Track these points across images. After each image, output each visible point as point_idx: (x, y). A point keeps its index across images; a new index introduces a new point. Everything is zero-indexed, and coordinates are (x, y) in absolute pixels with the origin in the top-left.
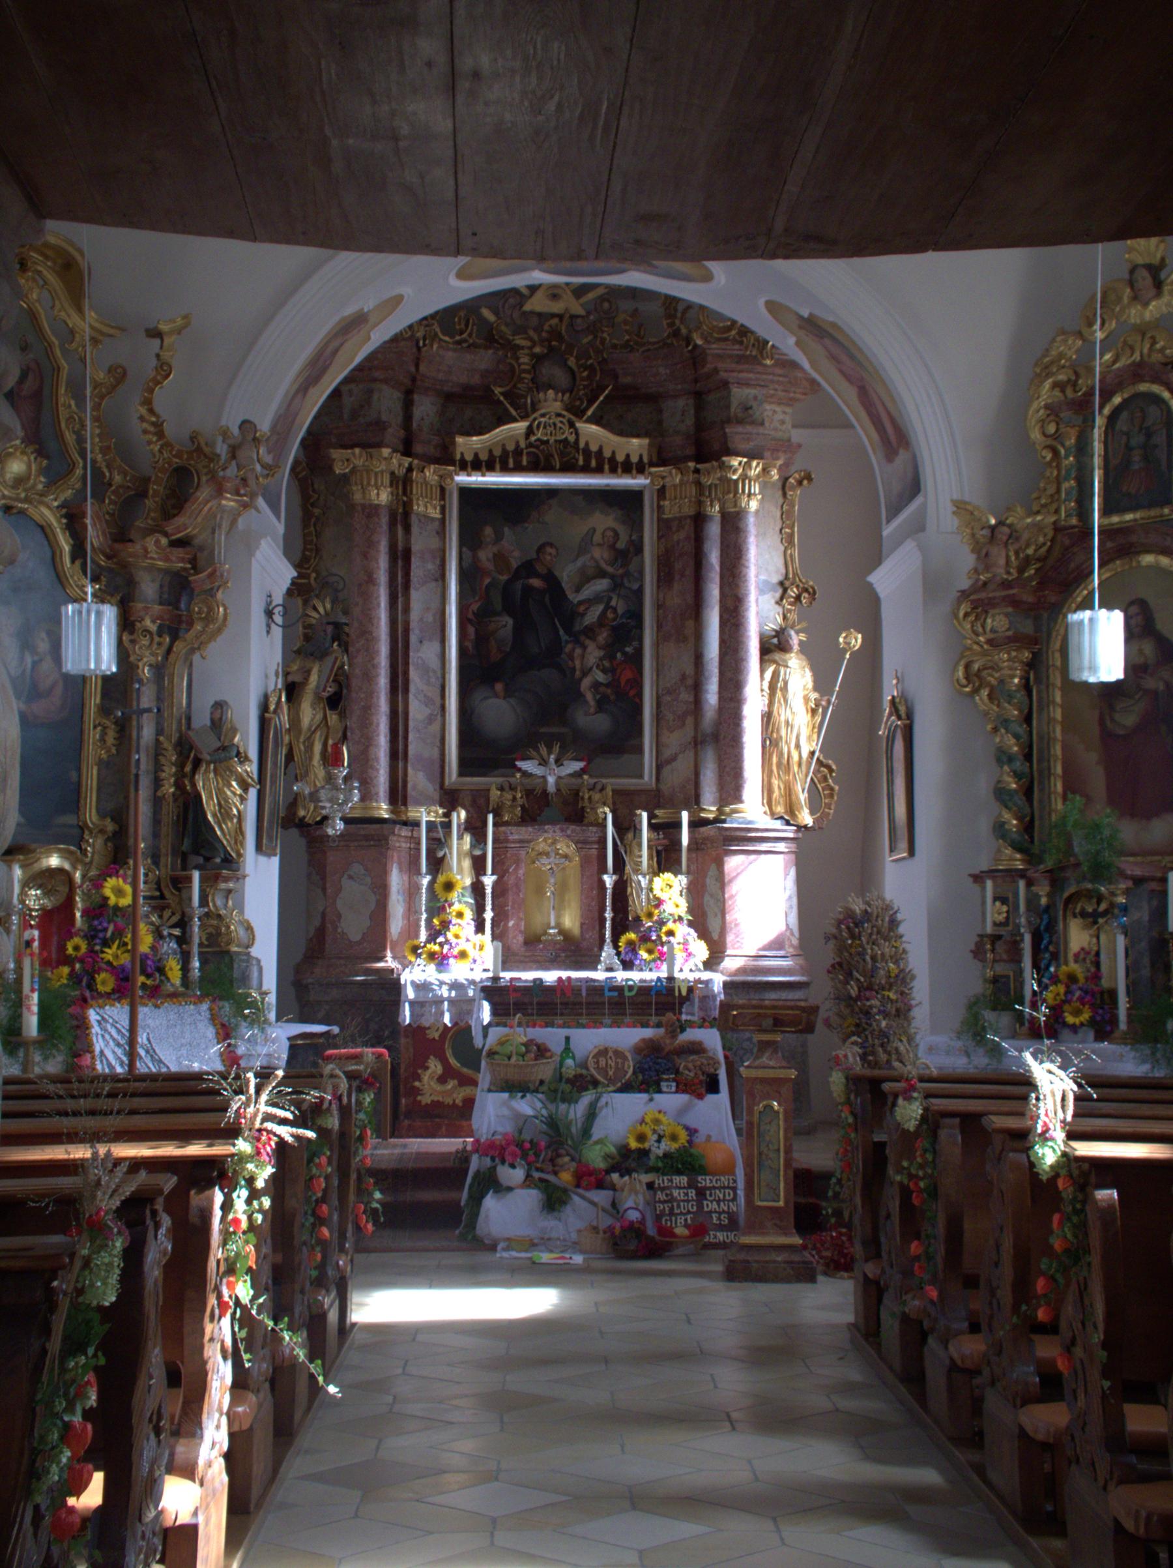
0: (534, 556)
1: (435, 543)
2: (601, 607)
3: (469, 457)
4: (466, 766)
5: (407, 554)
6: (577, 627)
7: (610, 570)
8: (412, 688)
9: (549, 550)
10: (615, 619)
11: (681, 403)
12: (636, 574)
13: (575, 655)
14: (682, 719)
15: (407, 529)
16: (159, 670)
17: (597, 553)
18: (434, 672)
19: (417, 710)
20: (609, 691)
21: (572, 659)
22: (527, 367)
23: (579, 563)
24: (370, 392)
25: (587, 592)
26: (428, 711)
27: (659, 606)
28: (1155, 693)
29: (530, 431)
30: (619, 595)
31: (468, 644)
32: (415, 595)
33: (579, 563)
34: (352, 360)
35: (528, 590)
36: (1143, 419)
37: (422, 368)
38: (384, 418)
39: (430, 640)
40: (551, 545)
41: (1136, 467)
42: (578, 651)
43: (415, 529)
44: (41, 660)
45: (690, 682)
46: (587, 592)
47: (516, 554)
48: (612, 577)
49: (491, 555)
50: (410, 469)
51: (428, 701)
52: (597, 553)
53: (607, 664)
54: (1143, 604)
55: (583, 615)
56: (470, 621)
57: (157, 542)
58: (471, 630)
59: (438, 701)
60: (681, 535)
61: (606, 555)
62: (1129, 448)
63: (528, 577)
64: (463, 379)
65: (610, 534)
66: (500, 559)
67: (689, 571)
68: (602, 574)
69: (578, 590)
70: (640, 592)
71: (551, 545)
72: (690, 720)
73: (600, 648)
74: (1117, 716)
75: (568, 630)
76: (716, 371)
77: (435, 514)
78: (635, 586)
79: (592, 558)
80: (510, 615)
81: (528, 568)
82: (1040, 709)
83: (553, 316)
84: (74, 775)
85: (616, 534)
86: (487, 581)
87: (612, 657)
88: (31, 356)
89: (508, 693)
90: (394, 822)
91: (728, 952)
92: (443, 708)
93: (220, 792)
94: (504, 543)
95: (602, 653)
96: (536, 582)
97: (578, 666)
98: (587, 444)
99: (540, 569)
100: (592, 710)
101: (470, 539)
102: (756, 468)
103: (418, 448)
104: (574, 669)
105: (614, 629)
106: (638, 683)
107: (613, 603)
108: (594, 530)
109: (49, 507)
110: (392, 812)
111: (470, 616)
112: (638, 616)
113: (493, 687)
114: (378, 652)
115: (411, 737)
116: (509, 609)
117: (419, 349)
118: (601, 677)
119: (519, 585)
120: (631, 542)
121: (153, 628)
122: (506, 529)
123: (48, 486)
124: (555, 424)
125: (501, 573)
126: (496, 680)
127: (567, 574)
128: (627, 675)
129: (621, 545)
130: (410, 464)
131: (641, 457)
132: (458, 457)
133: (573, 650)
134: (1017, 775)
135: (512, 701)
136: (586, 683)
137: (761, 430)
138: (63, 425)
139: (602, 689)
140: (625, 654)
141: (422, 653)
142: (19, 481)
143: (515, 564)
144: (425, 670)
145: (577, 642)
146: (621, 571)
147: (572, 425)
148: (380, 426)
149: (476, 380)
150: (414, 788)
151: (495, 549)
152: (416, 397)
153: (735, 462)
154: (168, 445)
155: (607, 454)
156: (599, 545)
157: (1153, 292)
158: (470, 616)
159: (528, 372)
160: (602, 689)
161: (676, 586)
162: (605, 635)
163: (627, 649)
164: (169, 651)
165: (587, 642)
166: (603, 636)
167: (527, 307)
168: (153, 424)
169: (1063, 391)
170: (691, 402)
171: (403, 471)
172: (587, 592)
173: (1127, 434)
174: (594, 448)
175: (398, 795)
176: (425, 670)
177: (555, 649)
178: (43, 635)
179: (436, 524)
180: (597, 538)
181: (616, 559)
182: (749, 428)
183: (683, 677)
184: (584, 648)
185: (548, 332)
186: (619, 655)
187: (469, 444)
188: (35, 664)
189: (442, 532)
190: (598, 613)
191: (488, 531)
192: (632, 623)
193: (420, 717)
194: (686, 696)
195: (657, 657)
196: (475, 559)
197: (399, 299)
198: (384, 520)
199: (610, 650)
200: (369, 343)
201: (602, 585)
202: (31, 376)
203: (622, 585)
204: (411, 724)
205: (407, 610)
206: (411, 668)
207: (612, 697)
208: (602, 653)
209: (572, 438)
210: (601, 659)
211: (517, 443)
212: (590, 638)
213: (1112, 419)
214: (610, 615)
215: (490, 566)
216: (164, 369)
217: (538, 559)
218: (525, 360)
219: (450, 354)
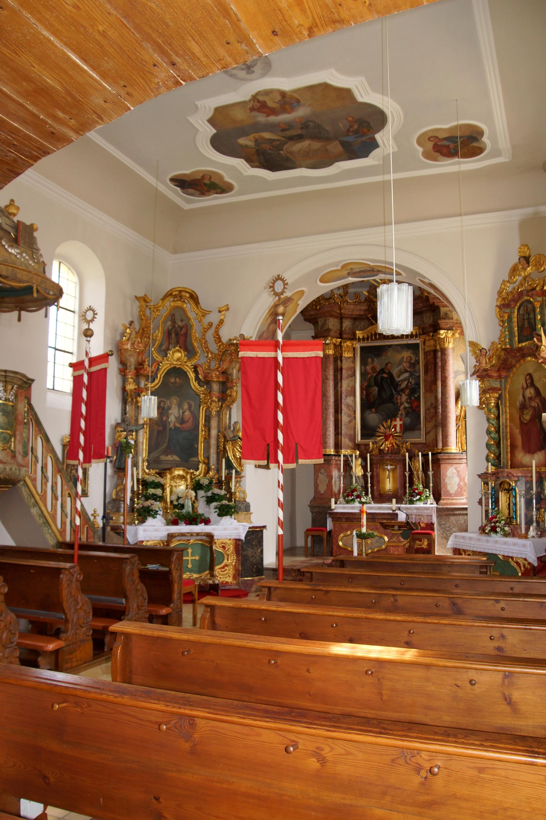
1: (351, 365)
2: (406, 382)
3: (361, 337)
4: (363, 436)
5: (341, 369)
6: (399, 389)
7: (409, 370)
8: (343, 412)
9: (389, 365)
14: (432, 418)
15: (341, 361)
16: (219, 413)
17: (405, 364)
18: (351, 406)
19: (345, 418)
23: (399, 368)
24: (326, 320)
26: (349, 419)
27: (425, 381)
28: (534, 407)
30: (412, 378)
31: (364, 397)
32: (343, 382)
33: (399, 368)
34: (296, 311)
35: (382, 378)
36: (527, 309)
37: (342, 311)
38: (330, 327)
39: (350, 396)
40: (390, 363)
41: (526, 326)
42: (399, 397)
43: (344, 361)
44: (185, 412)
45: (433, 406)
47: (379, 367)
48: (410, 372)
50: (341, 342)
51: (349, 416)
52: (405, 364)
53: (409, 401)
54: (530, 375)
55: (401, 385)
57: (216, 374)
58: (364, 392)
59: (353, 416)
60: (430, 357)
61: (408, 365)
62: (524, 320)
64: (358, 313)
65: (409, 358)
66: (373, 368)
67: (433, 369)
68: (406, 371)
69: (399, 377)
70: (419, 376)
71: (390, 363)
72: (434, 419)
73: (406, 395)
74: (524, 416)
75: (396, 390)
76: (434, 303)
77: (350, 355)
78: (418, 375)
79: (403, 366)
81: (382, 371)
82: (502, 414)
84: (196, 446)
85: (411, 358)
86: (369, 376)
87: (410, 398)
88: (184, 323)
89: (376, 412)
90: (334, 455)
91: (442, 498)
92: (355, 418)
93: (233, 450)
94: (375, 363)
95: (407, 397)
96: (385, 375)
99: (386, 371)
101: (363, 363)
102: (450, 333)
103: (345, 336)
105: (411, 389)
106: (419, 406)
107: (410, 381)
108: (404, 357)
109: (187, 366)
110: (336, 452)
111: (364, 387)
112: (419, 385)
114: (329, 401)
115: (343, 427)
116: (376, 384)
117: (340, 306)
118: (407, 405)
119: (379, 377)
120: (416, 360)
121: (216, 400)
123: (187, 360)
125: (374, 373)
126: (373, 407)
127: (395, 372)
128: (415, 404)
129: (413, 361)
132: (357, 337)
134: (493, 439)
135: (378, 414)
136: (402, 407)
137: (451, 321)
138: (193, 341)
139: (407, 409)
140: (414, 397)
141: (346, 400)
142: (178, 360)
143: (378, 370)
144: (348, 406)
145: (399, 394)
148: (329, 330)
149: (362, 313)
150: (344, 444)
151: (372, 365)
152: (344, 320)
153: (442, 332)
154: (223, 344)
156: (405, 362)
157: (527, 265)
158: (364, 387)
160: (407, 409)
161: (429, 374)
164: (222, 406)
165: (402, 394)
166: (407, 392)
168: (218, 338)
169: (505, 301)
172: (401, 378)
173: (523, 315)
175: (338, 446)
176: (348, 406)
177: (392, 396)
178: (186, 404)
179: (352, 359)
180: (405, 360)
181: (411, 366)
182: (447, 321)
183: (432, 404)
184: (401, 396)
186: (413, 398)
187: (359, 334)
188: (183, 413)
189: (354, 362)
191: (370, 360)
192: (417, 387)
193: (346, 421)
194: (433, 411)
195: (425, 397)
196: (366, 369)
197: (302, 292)
198: (332, 359)
199: (410, 396)
200: (299, 307)
201: (406, 375)
202: (184, 329)
203: (413, 375)
204: (343, 423)
205: (341, 387)
206: (343, 406)
208: (407, 397)
210: (407, 399)
212: (402, 392)
213: (519, 309)
214: (409, 384)
215: (370, 371)
216: (221, 322)
217: (386, 368)
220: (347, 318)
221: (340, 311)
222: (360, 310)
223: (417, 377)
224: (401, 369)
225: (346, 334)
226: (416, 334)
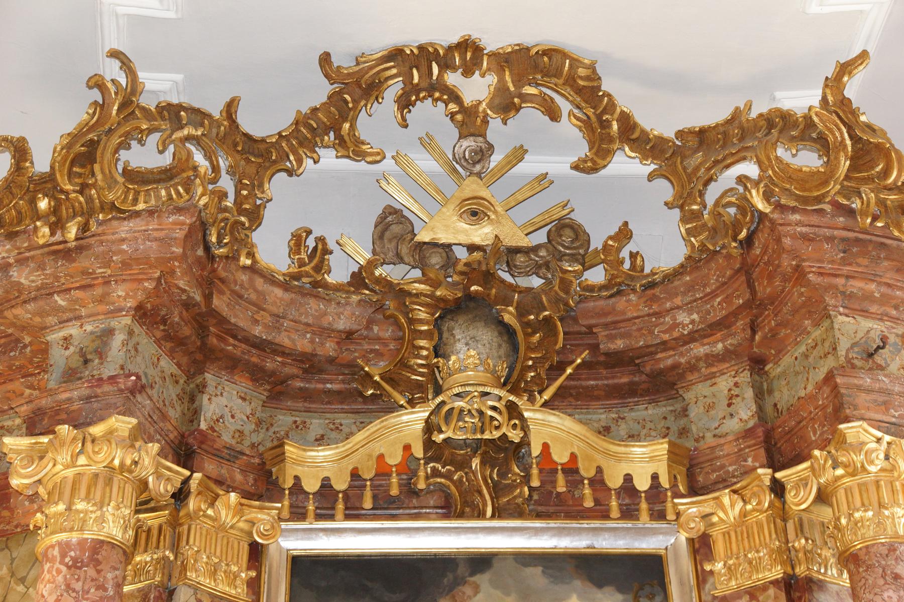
11: (724, 384)
22: (425, 328)
29: (430, 428)
50: (181, 495)
64: (303, 343)
83: (472, 248)
98: (546, 446)
124: (481, 413)
130: (186, 481)
131: (655, 477)
132: (289, 483)
147: (513, 410)
149: (329, 348)
155: (587, 471)
159: (427, 335)
167: (424, 236)
170: (745, 377)
171: (162, 488)
174: (560, 456)
185: (462, 273)
209: (515, 436)
211: (407, 448)
218: (422, 314)
219: (278, 292)
220: (233, 365)
221: (208, 297)
222: (325, 332)
225: (216, 454)
226: (656, 491)
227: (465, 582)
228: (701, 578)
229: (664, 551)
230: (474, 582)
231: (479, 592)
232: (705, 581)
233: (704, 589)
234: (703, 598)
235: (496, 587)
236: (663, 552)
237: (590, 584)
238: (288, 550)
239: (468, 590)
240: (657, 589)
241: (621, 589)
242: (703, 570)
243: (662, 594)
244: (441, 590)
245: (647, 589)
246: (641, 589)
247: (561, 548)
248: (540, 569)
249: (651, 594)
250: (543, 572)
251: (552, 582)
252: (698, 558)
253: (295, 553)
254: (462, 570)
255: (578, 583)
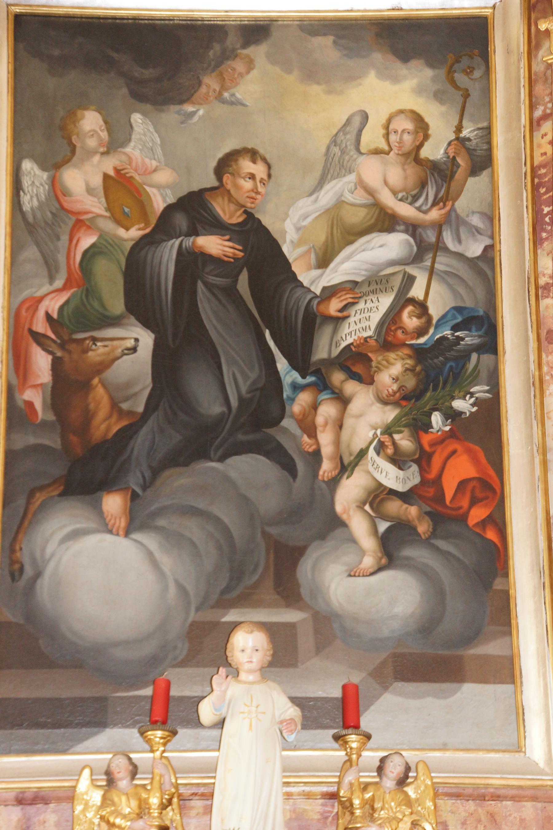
0: (211, 181)
10: (421, 332)
12: (476, 221)
13: (320, 420)
20: (413, 511)
21: (312, 432)
25: (348, 266)
30: (432, 271)
46: (348, 266)
49: (97, 181)
56: (39, 338)
63: (194, 232)
73: (385, 402)
79: (361, 184)
80: (146, 324)
97: (327, 450)
100: (368, 562)
104: (317, 455)
108: (365, 117)
113: (97, 507)
120: (461, 141)
122: (137, 118)
133: (315, 407)
146: (435, 214)
156: (377, 152)
162: (397, 369)
163: (459, 404)
181: (423, 185)
186: (436, 419)
190: (376, 318)
207: (423, 528)
210: (389, 430)
223: (472, 262)
224: (340, 204)
227: (236, 56)
228: (533, 43)
229: (491, 11)
230: (248, 56)
231: (252, 69)
232: (538, 46)
233: (536, 56)
234: (534, 68)
235: (274, 62)
236: (488, 12)
237: (392, 57)
238: (8, 5)
239: (239, 66)
240: (478, 60)
241: (431, 64)
242: (538, 30)
243: (483, 68)
244: (205, 65)
245: (465, 62)
246: (458, 61)
247: (358, 11)
248: (331, 38)
249: (469, 68)
250: (334, 42)
251: (345, 55)
252: (533, 16)
253: (17, 10)
254: (232, 40)
255: (377, 57)
